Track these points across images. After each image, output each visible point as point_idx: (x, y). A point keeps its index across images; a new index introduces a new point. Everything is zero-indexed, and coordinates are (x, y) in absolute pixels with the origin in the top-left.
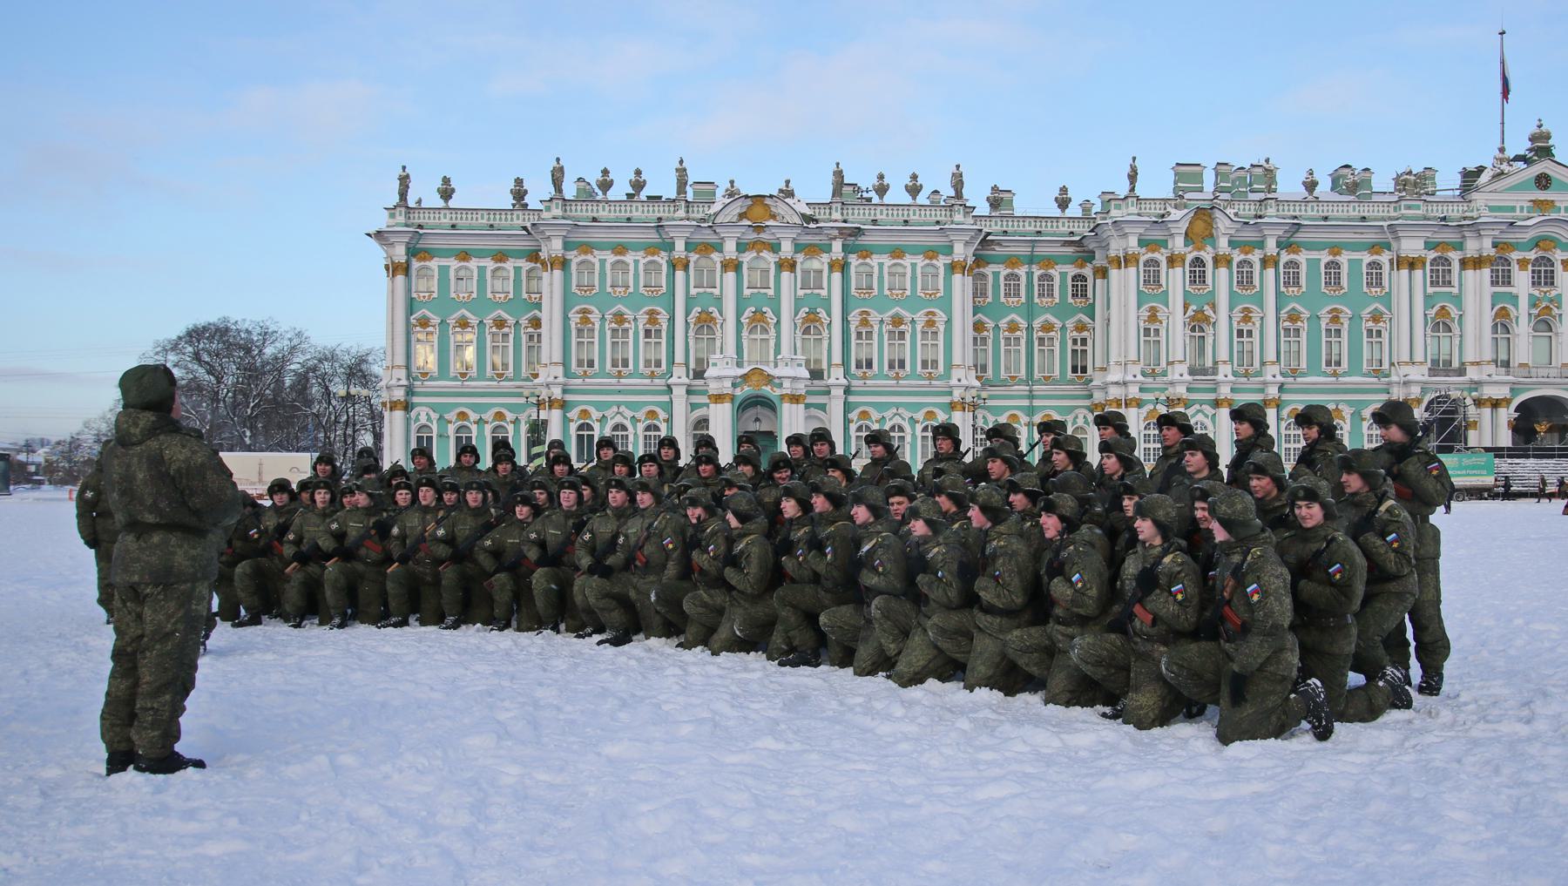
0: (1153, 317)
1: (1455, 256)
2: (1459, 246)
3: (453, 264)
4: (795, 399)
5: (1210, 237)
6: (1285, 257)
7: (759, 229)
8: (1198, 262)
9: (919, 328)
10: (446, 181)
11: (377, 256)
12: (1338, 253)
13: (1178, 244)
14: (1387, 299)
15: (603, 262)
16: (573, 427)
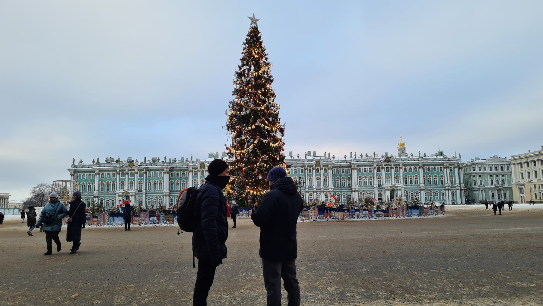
3: (82, 174)
11: (69, 173)
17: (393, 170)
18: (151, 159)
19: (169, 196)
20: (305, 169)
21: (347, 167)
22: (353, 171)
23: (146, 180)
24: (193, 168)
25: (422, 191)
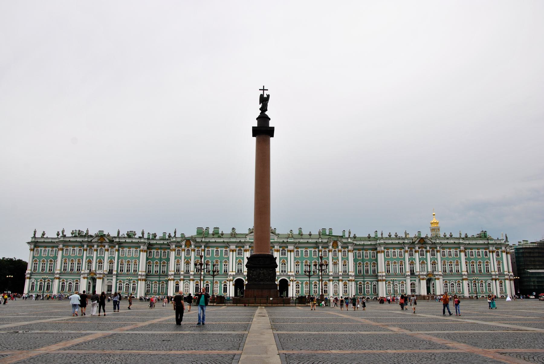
0: (178, 262)
1: (242, 249)
2: (243, 247)
3: (43, 249)
4: (100, 278)
5: (191, 245)
6: (206, 249)
7: (101, 243)
8: (188, 250)
10: (44, 232)
11: (28, 247)
13: (183, 246)
14: (228, 258)
16: (61, 283)
17: (428, 254)
18: (125, 233)
19: (145, 280)
20: (319, 251)
21: (372, 249)
22: (379, 254)
23: (118, 260)
24: (176, 246)
25: (464, 281)
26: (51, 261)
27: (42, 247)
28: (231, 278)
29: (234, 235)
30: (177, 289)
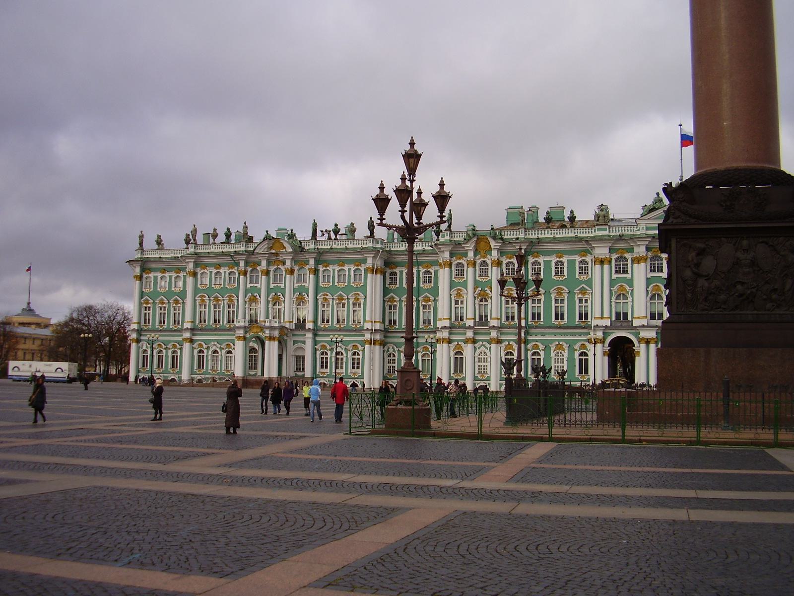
1: (627, 256)
2: (631, 250)
3: (159, 275)
4: (271, 339)
5: (489, 250)
7: (277, 254)
8: (484, 263)
9: (351, 301)
10: (159, 237)
12: (563, 257)
13: (471, 254)
14: (589, 283)
15: (211, 273)
16: (196, 351)
18: (331, 228)
19: (383, 344)
23: (316, 294)
24: (452, 255)
26: (177, 302)
27: (156, 270)
28: (600, 334)
29: (603, 217)
30: (459, 364)
